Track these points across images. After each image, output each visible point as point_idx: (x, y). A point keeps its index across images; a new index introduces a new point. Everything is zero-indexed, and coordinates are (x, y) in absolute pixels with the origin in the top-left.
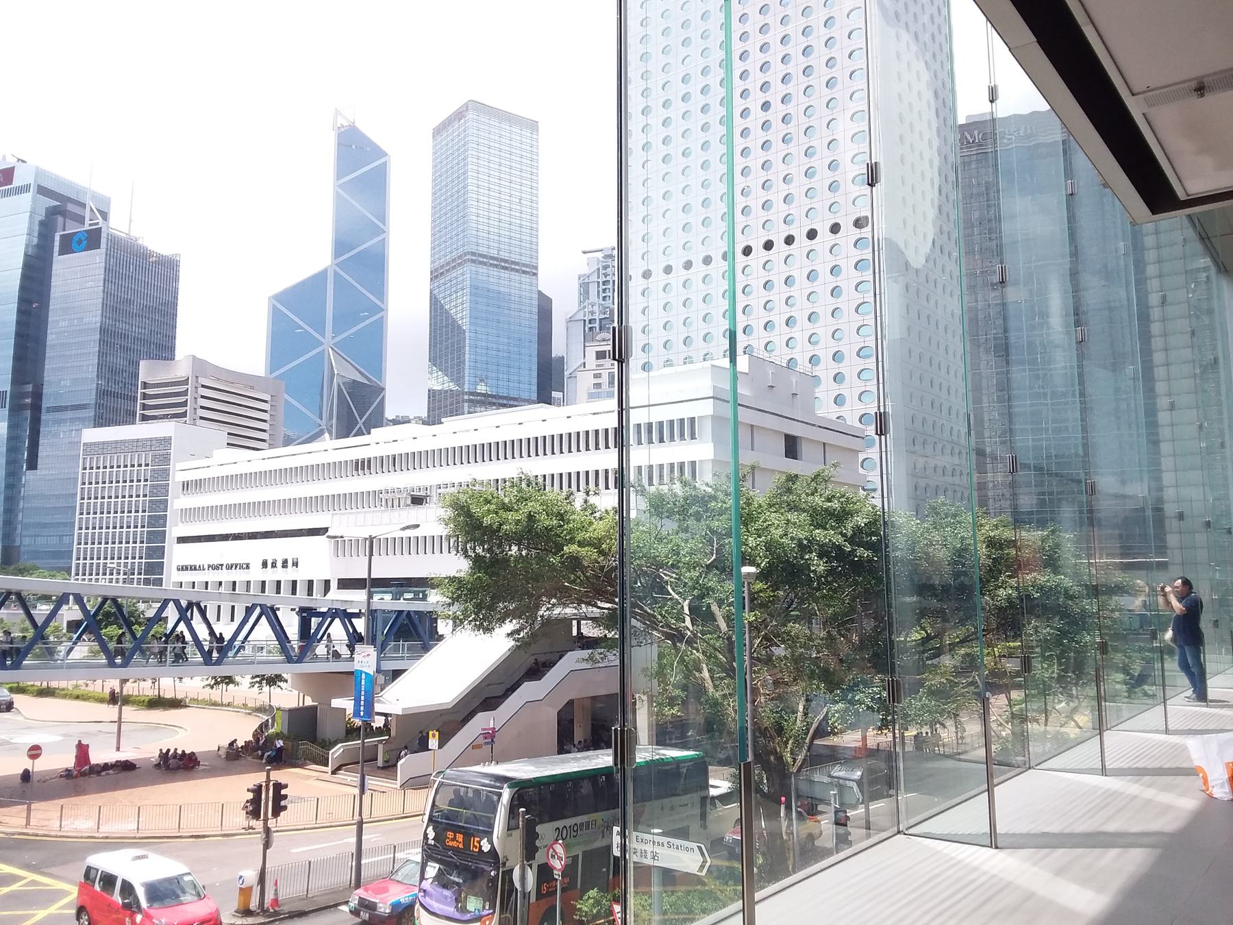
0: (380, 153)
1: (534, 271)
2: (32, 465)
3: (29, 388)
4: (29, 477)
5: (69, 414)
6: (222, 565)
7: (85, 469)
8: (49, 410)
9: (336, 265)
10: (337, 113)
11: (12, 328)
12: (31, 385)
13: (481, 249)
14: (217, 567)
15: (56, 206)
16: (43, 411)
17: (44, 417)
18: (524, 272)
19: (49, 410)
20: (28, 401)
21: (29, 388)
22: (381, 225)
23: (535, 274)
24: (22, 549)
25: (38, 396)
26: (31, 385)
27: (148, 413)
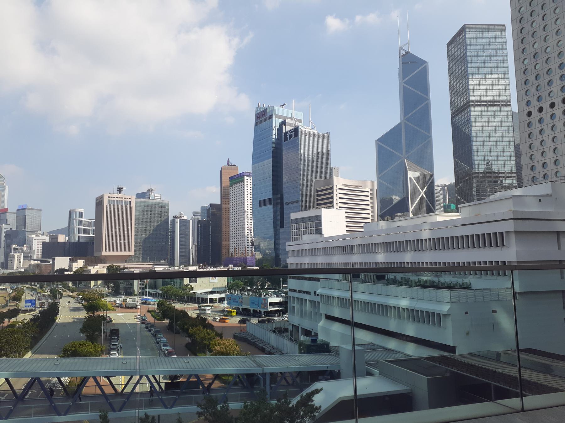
0: (423, 62)
1: (509, 104)
2: (282, 226)
3: (279, 196)
4: (281, 230)
5: (292, 205)
6: (302, 291)
7: (292, 230)
8: (288, 203)
9: (405, 120)
10: (401, 49)
11: (271, 173)
12: (279, 195)
13: (476, 98)
14: (300, 292)
15: (283, 121)
16: (284, 204)
17: (285, 207)
18: (503, 105)
19: (288, 203)
20: (279, 201)
21: (279, 196)
22: (425, 96)
23: (510, 105)
24: (281, 259)
25: (282, 198)
26: (279, 195)
27: (319, 202)
